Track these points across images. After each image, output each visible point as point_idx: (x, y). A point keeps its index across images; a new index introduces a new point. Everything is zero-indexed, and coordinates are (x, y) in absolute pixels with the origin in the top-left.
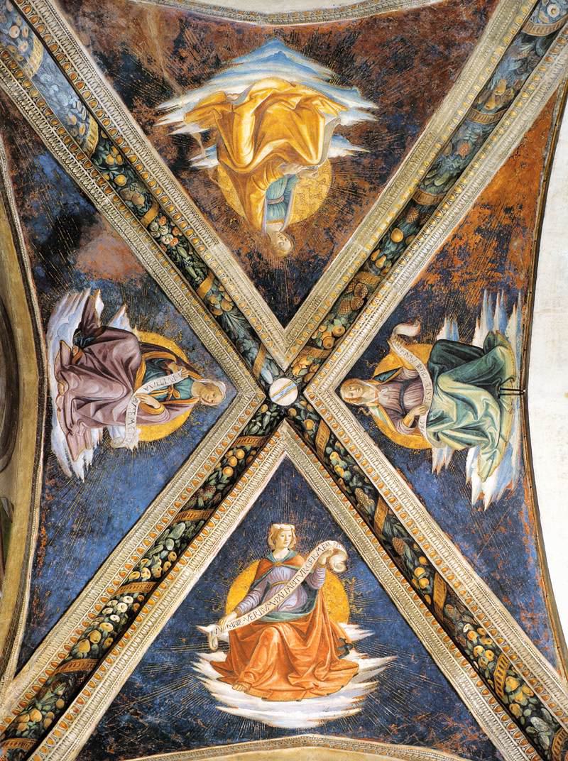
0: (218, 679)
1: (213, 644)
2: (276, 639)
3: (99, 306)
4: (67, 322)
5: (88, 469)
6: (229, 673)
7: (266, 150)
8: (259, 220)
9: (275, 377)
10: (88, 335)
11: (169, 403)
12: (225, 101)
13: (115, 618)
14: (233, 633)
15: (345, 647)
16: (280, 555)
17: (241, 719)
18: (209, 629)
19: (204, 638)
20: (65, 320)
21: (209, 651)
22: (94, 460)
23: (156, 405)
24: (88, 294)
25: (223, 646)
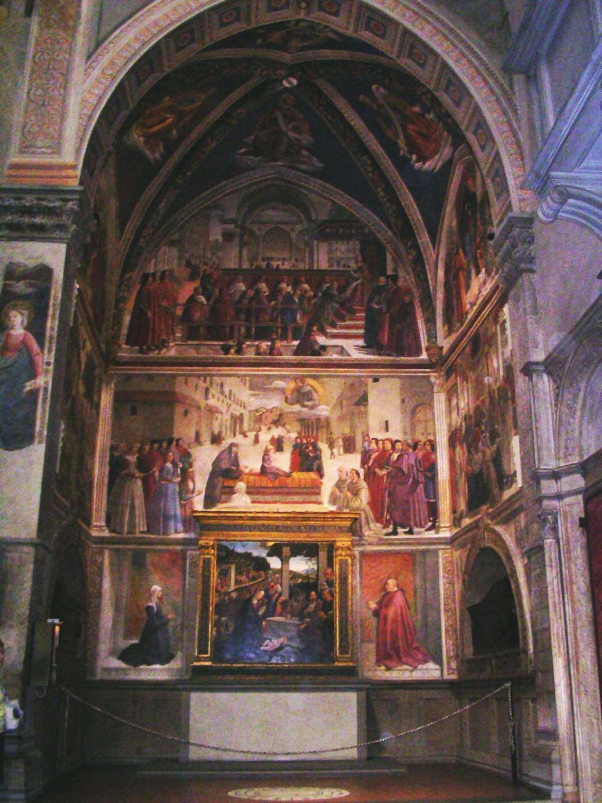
0: (424, 164)
1: (409, 157)
2: (413, 133)
3: (243, 150)
4: (251, 159)
5: (320, 162)
6: (423, 158)
7: (167, 115)
8: (200, 103)
9: (282, 85)
10: (256, 150)
11: (289, 119)
12: (147, 142)
13: (385, 199)
14: (406, 145)
15: (422, 115)
16: (375, 107)
17: (442, 168)
18: (402, 153)
19: (404, 156)
20: (249, 162)
21: (411, 159)
22: (317, 157)
23: (293, 123)
24: (237, 156)
25: (411, 153)
